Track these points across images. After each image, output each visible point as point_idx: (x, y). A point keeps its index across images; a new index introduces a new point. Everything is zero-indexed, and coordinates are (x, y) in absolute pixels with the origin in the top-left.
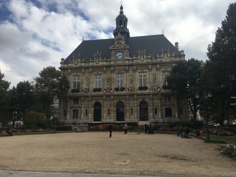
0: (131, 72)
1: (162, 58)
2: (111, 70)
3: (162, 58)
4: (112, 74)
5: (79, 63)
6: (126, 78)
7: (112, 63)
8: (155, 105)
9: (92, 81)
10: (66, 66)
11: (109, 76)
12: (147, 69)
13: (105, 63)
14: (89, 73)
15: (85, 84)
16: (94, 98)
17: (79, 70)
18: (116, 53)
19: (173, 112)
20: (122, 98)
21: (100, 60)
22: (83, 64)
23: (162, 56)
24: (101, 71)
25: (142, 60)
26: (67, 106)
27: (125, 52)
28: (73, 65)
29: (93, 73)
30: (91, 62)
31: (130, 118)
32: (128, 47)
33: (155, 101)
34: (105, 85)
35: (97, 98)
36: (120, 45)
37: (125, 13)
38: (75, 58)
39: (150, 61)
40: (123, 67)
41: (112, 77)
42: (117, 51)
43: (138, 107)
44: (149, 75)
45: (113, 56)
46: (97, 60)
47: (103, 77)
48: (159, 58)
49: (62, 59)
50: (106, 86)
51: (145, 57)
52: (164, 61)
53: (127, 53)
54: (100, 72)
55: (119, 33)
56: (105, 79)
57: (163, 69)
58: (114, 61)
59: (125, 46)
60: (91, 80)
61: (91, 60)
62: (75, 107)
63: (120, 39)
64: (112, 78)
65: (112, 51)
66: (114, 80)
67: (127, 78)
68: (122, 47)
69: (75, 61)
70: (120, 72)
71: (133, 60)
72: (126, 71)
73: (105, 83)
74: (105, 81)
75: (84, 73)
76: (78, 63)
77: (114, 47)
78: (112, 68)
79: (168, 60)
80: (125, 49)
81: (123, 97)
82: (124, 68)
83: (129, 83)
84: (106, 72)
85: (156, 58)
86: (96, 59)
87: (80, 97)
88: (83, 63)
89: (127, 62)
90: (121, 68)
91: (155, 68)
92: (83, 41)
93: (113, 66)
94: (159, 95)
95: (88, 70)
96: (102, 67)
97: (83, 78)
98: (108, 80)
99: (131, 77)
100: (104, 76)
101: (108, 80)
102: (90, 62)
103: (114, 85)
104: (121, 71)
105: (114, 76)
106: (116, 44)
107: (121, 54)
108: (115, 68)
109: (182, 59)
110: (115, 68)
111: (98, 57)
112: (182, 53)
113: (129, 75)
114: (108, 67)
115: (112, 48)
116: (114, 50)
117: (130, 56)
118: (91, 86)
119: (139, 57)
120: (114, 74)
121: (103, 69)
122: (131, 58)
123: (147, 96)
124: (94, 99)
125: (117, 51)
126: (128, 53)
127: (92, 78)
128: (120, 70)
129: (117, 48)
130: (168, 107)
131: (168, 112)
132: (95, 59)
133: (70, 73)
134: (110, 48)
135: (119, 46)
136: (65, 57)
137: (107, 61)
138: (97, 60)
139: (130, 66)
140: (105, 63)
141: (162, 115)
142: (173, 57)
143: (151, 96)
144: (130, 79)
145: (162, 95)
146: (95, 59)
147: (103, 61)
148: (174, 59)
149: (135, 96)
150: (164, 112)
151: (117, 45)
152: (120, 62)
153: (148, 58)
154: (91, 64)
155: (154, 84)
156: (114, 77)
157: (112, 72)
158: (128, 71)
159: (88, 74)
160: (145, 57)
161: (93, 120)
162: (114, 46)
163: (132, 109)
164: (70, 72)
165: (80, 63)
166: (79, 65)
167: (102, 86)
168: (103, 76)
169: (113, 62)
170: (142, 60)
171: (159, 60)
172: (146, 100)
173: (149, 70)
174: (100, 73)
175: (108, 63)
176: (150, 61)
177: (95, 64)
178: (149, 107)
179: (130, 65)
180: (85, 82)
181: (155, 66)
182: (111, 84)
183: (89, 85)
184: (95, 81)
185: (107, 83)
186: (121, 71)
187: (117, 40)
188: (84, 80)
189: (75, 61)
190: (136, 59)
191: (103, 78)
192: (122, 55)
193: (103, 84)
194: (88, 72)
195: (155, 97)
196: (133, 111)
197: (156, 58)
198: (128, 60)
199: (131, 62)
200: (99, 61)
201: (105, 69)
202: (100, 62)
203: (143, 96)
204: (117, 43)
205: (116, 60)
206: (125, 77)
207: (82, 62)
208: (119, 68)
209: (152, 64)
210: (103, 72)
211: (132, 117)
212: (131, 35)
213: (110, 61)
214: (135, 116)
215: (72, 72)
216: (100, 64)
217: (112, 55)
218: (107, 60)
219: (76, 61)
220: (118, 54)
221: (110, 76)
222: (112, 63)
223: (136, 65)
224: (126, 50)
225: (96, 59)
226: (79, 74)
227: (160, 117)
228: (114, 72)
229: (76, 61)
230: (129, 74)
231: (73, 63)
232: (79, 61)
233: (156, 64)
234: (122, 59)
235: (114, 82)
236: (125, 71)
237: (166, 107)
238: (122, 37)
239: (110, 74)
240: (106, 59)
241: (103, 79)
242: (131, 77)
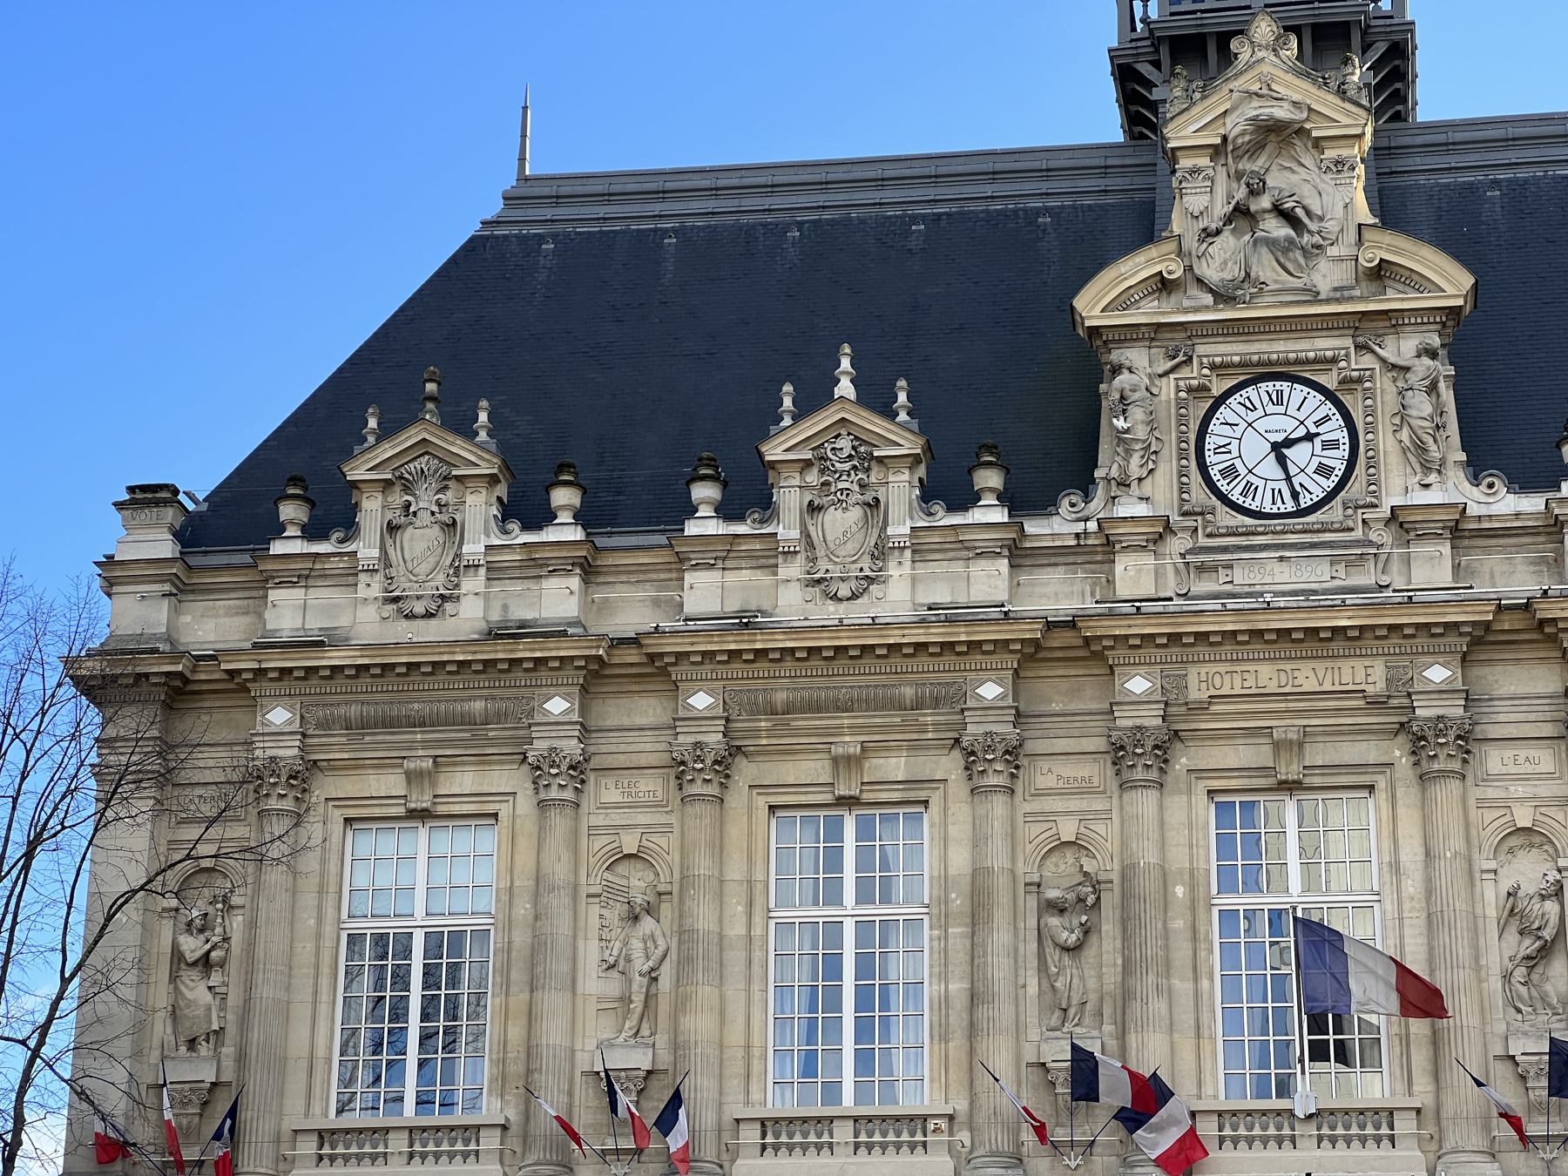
2: (1126, 719)
4: (1145, 803)
5: (473, 584)
6: (1429, 891)
9: (736, 929)
10: (212, 627)
11: (1068, 831)
13: (988, 581)
14: (679, 769)
15: (594, 983)
17: (478, 706)
18: (1201, 390)
21: (899, 529)
22: (558, 599)
24: (915, 747)
27: (1384, 385)
28: (357, 617)
29: (746, 772)
34: (1004, 1011)
36: (1280, 249)
38: (407, 489)
41: (1148, 856)
42: (1232, 350)
45: (1150, 453)
47: (960, 860)
49: (147, 498)
50: (1019, 1029)
53: (1421, 405)
54: (884, 748)
55: (1264, 29)
56: (1002, 883)
58: (1177, 544)
59: (1381, 273)
60: (703, 917)
61: (714, 527)
63: (1275, 135)
64: (1128, 872)
65: (1136, 356)
66: (1179, 924)
67: (1449, 873)
68: (1327, 275)
69: (392, 528)
70: (1290, 771)
72: (1419, 741)
73: (999, 969)
74: (1000, 938)
75: (578, 770)
76: (460, 568)
77: (1163, 285)
78: (1138, 685)
80: (1393, 321)
82: (1377, 686)
83: (1495, 984)
84: (1013, 754)
86: (814, 509)
88: (553, 584)
90: (1308, 676)
92: (523, 179)
95: (647, 709)
96: (952, 645)
97: (559, 870)
98: (1059, 908)
99: (1529, 872)
100: (978, 841)
101: (1059, 908)
103: (1186, 1018)
104: (1318, 754)
105: (1172, 829)
106: (1208, 235)
107: (1304, 405)
108: (1201, 680)
110: (1194, 675)
111: (865, 459)
113: (1490, 824)
115: (1122, 303)
116: (1175, 340)
117: (1476, 468)
118: (699, 1025)
120: (1176, 806)
121: (954, 700)
122: (1507, 504)
125: (1232, 350)
126: (1448, 395)
127: (735, 870)
128: (1287, 728)
129: (1223, 296)
133: (302, 776)
134: (1079, 303)
135: (1266, 268)
136: (200, 476)
137: (1019, 554)
138: (841, 522)
139: (1509, 643)
140: (988, 581)
144: (1513, 910)
151: (1227, 244)
152: (1281, 577)
156: (1178, 858)
157: (1140, 756)
158: (1467, 740)
159: (650, 786)
162: (1175, 270)
164: (288, 751)
165: (495, 572)
166: (472, 611)
167: (942, 1035)
168: (960, 829)
169: (1148, 560)
174: (895, 766)
175: (1057, 593)
177: (790, 602)
179: (1480, 641)
180: (591, 954)
182: (1126, 995)
183: (681, 1005)
184: (785, 927)
185: (1033, 989)
186: (1318, 754)
187: (1217, 151)
188: (558, 903)
189: (392, 528)
191: (944, 881)
192: (1335, 429)
193: (958, 987)
194: (649, 748)
198: (1460, 530)
200: (881, 552)
201: (990, 691)
202: (898, 570)
204: (1221, 208)
205: (1217, 516)
206: (1396, 868)
207: (536, 565)
208: (1266, 675)
210: (948, 766)
212: (1438, 97)
213: (1101, 549)
215: (334, 747)
216: (900, 596)
217: (1120, 437)
218: (1032, 527)
219: (420, 541)
220: (1247, 434)
221: (1106, 834)
222: (1134, 575)
224: (1403, 347)
225: (814, 509)
226: (462, 781)
228: (1182, 761)
230: (1482, 803)
231: (351, 574)
232: (473, 548)
234: (1334, 512)
235: (1181, 952)
236: (1398, 752)
238: (1325, 102)
239: (1098, 804)
240: (1019, 501)
241: (958, 901)
242: (1529, 872)
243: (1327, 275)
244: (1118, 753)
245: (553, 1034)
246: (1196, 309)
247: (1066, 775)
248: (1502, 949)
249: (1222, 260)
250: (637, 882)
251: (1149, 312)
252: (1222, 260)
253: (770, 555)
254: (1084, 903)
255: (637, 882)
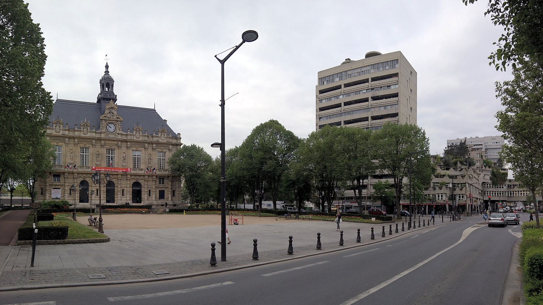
0: (124, 149)
1: (159, 137)
3: (159, 137)
7: (103, 136)
8: (150, 187)
12: (142, 147)
13: (94, 134)
16: (81, 175)
19: (165, 194)
20: (113, 177)
22: (67, 132)
23: (160, 135)
25: (138, 136)
26: (45, 183)
30: (78, 131)
31: (120, 200)
32: (122, 119)
33: (150, 183)
35: (85, 175)
37: (112, 74)
39: (146, 139)
40: (116, 143)
43: (131, 188)
44: (142, 154)
46: (85, 130)
48: (156, 137)
51: (141, 134)
52: (161, 141)
57: (160, 150)
62: (57, 185)
68: (115, 117)
71: (127, 135)
79: (165, 141)
81: (115, 176)
85: (153, 137)
87: (64, 173)
89: (119, 137)
91: (151, 148)
93: (105, 140)
94: (155, 177)
102: (75, 131)
108: (106, 142)
109: (178, 142)
112: (178, 136)
114: (100, 139)
119: (134, 133)
121: (92, 142)
123: (142, 177)
124: (80, 177)
130: (162, 189)
131: (162, 195)
132: (82, 128)
137: (96, 133)
138: (85, 130)
140: (94, 135)
141: (156, 198)
142: (170, 138)
143: (147, 177)
145: (157, 176)
146: (82, 128)
147: (92, 132)
148: (171, 140)
149: (129, 176)
150: (158, 194)
151: (109, 114)
152: (111, 136)
153: (145, 136)
154: (76, 134)
155: (150, 165)
157: (102, 146)
160: (141, 134)
161: (78, 201)
163: (123, 190)
166: (61, 133)
170: (138, 136)
171: (155, 139)
172: (141, 181)
173: (145, 148)
175: (98, 136)
176: (146, 139)
177: (82, 135)
178: (143, 189)
179: (123, 141)
181: (151, 145)
190: (131, 135)
194: (73, 143)
195: (150, 179)
196: (125, 192)
197: (153, 137)
198: (121, 134)
199: (124, 138)
203: (138, 177)
207: (65, 130)
208: (110, 142)
209: (149, 143)
211: (123, 199)
213: (101, 133)
214: (128, 198)
215: (52, 141)
216: (89, 135)
219: (58, 127)
223: (131, 141)
224: (119, 123)
226: (60, 144)
227: (154, 199)
229: (58, 127)
231: (53, 129)
233: (152, 143)
237: (160, 189)
242: (124, 155)
243: (115, 117)
244: (101, 146)
245: (67, 160)
246: (107, 118)
247: (98, 146)
248: (122, 159)
249: (109, 115)
250: (71, 151)
251: (104, 118)
252: (109, 115)
253: (81, 131)
254: (98, 155)
255: (71, 151)
